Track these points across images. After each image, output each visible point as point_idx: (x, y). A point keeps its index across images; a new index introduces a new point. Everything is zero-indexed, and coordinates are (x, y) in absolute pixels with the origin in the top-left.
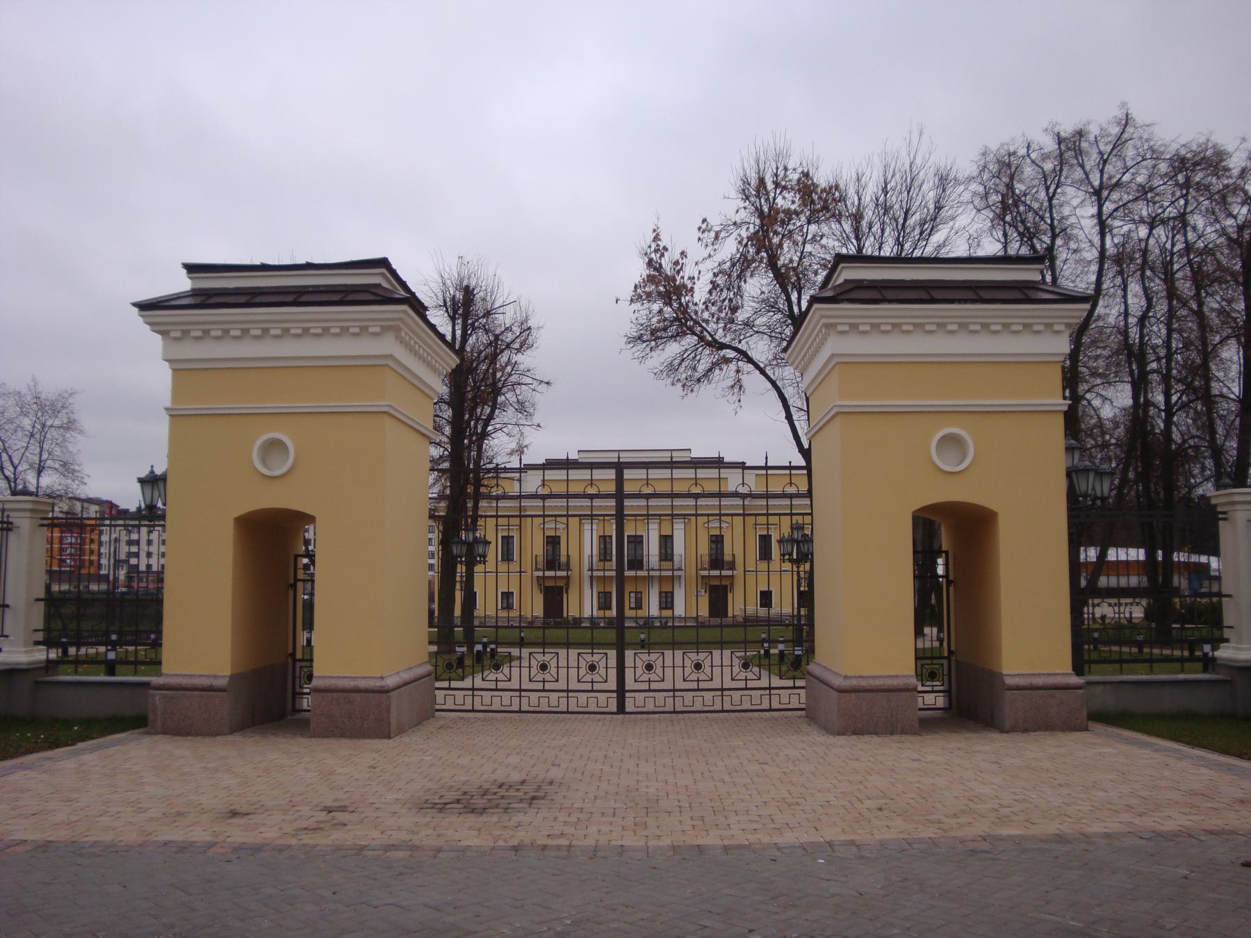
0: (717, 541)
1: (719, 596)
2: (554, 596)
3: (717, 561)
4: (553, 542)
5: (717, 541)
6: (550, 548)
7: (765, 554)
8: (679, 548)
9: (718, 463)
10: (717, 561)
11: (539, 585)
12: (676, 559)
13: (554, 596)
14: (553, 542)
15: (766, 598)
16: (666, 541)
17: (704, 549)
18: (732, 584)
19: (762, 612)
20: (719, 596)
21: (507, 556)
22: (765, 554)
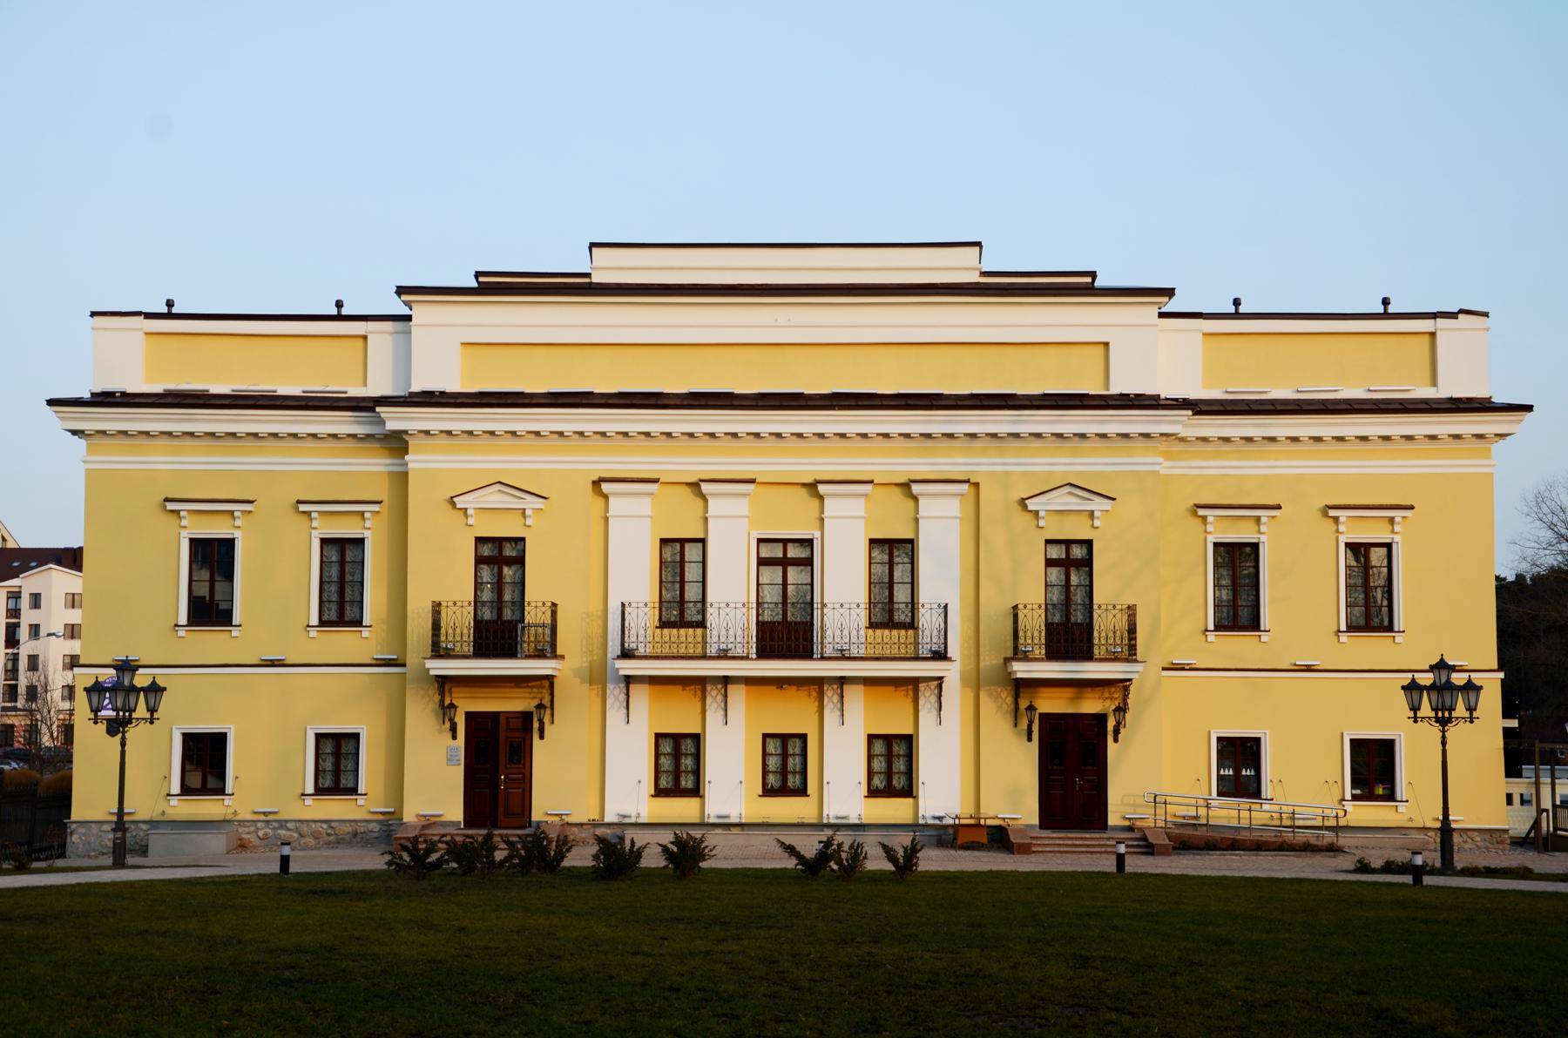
0: (1073, 560)
1: (1073, 759)
2: (497, 755)
3: (1070, 635)
4: (501, 557)
5: (1073, 560)
6: (486, 573)
7: (1239, 606)
8: (939, 582)
9: (1079, 287)
10: (1070, 635)
11: (447, 710)
12: (928, 620)
13: (497, 755)
14: (501, 557)
15: (1240, 760)
16: (894, 553)
17: (1031, 589)
18: (1121, 710)
19: (1229, 813)
20: (1073, 759)
21: (340, 606)
22: (1239, 606)
